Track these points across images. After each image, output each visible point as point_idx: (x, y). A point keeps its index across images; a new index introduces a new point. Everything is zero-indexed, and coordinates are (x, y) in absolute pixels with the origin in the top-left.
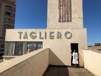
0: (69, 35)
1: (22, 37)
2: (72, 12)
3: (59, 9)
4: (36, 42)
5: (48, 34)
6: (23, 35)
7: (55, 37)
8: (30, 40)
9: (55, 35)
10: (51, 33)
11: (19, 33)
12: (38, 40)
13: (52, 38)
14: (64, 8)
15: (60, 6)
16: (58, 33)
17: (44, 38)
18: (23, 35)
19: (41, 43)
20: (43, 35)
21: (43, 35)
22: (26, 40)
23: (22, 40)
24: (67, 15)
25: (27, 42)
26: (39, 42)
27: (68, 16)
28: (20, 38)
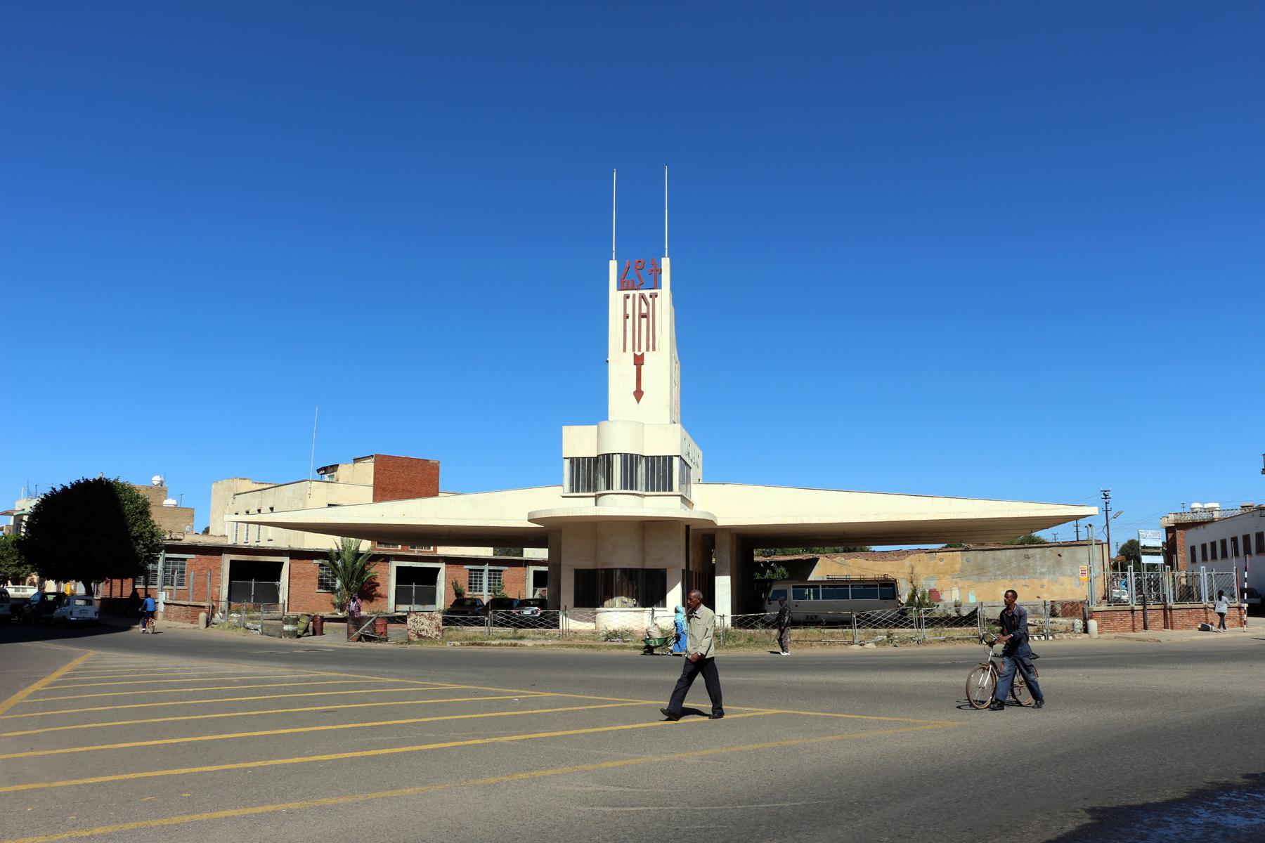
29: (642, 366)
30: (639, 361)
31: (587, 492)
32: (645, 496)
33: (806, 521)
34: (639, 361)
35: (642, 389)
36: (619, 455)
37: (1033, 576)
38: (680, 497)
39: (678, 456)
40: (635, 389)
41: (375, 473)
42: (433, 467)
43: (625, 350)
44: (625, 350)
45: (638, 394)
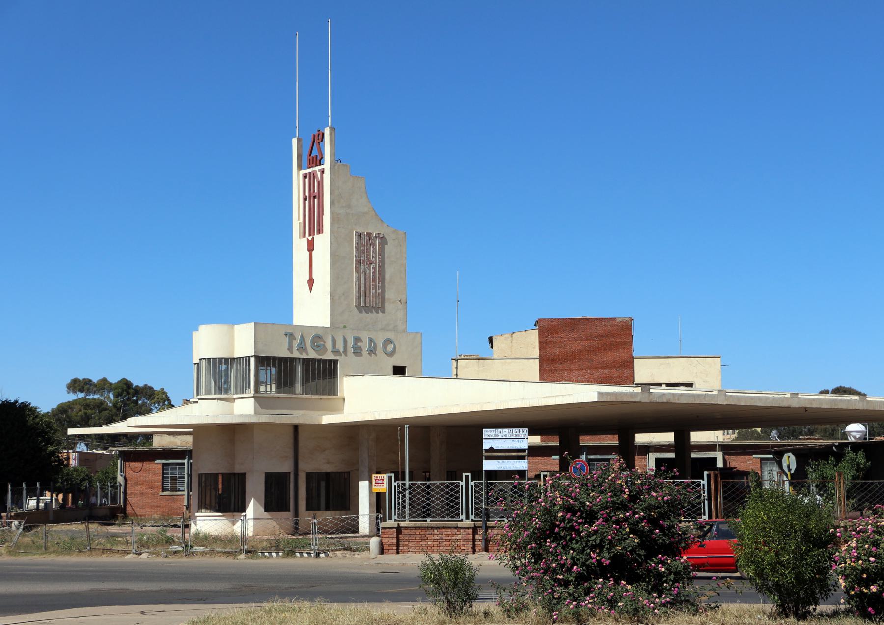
0: (390, 348)
1: (295, 349)
2: (386, 285)
3: (357, 271)
4: (325, 361)
5: (350, 343)
6: (296, 343)
7: (365, 352)
8: (312, 355)
9: (365, 345)
10: (357, 339)
11: (286, 335)
12: (329, 356)
13: (358, 352)
14: (367, 271)
15: (358, 262)
16: (371, 340)
17: (342, 350)
18: (296, 343)
19: (336, 362)
20: (340, 346)
21: (340, 346)
22: (304, 356)
23: (296, 354)
24: (373, 291)
25: (304, 359)
26: (330, 361)
27: (376, 292)
28: (290, 349)
29: (313, 251)
30: (311, 246)
31: (218, 394)
32: (235, 399)
33: (377, 418)
34: (311, 246)
35: (313, 278)
36: (204, 360)
37: (212, 488)
38: (253, 399)
39: (252, 356)
40: (308, 279)
41: (540, 342)
42: (622, 327)
43: (304, 236)
44: (304, 236)
45: (311, 282)
